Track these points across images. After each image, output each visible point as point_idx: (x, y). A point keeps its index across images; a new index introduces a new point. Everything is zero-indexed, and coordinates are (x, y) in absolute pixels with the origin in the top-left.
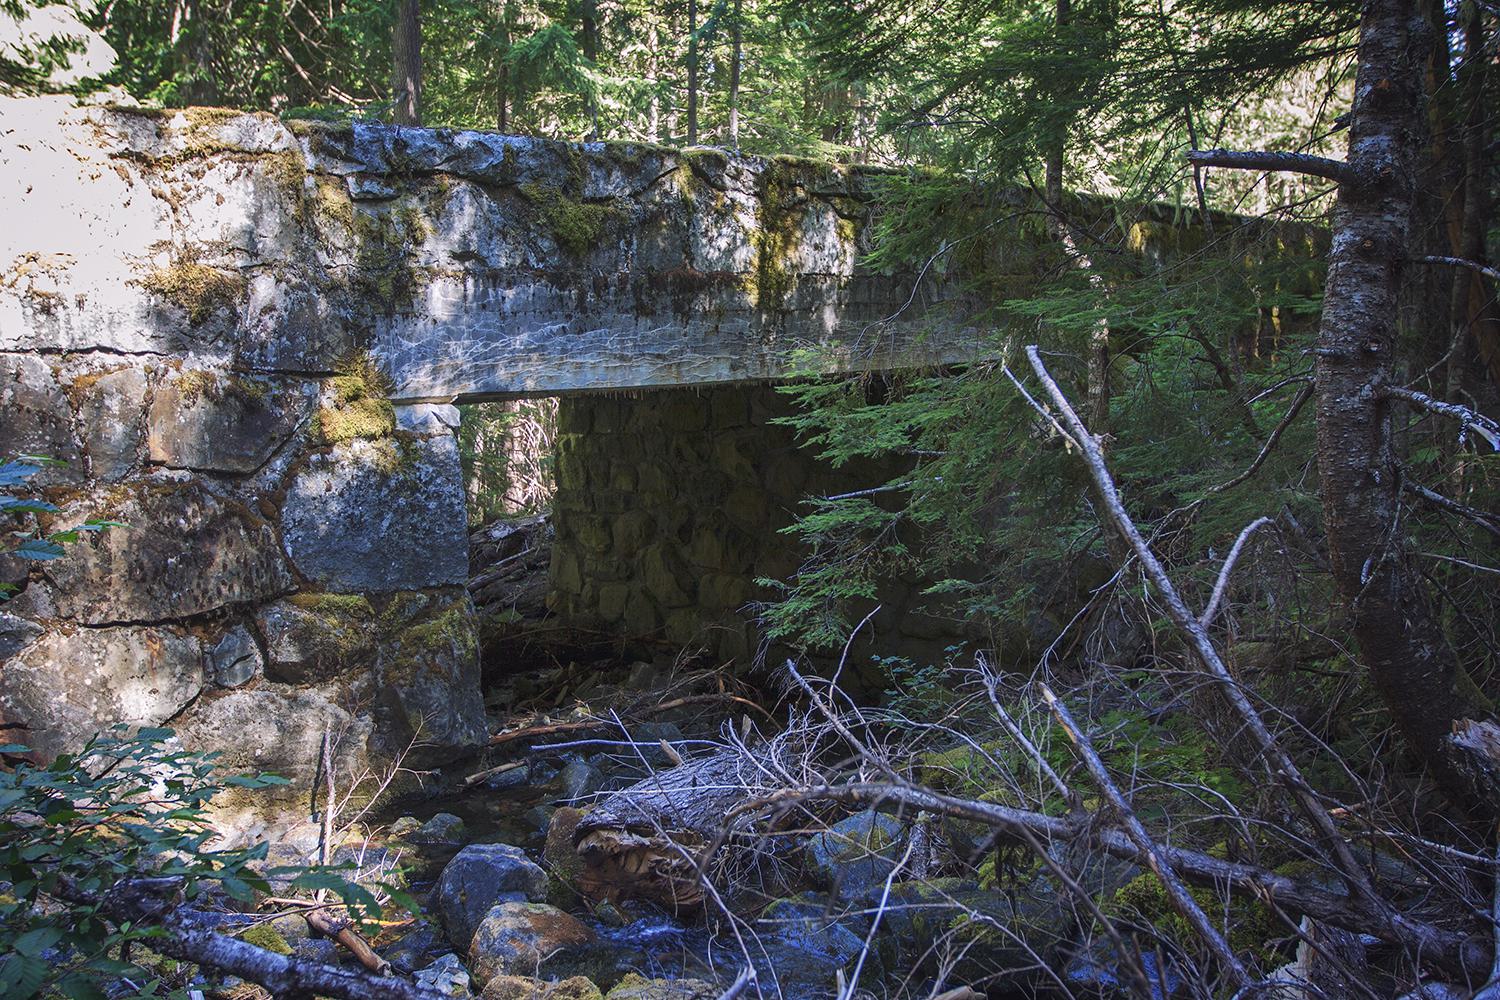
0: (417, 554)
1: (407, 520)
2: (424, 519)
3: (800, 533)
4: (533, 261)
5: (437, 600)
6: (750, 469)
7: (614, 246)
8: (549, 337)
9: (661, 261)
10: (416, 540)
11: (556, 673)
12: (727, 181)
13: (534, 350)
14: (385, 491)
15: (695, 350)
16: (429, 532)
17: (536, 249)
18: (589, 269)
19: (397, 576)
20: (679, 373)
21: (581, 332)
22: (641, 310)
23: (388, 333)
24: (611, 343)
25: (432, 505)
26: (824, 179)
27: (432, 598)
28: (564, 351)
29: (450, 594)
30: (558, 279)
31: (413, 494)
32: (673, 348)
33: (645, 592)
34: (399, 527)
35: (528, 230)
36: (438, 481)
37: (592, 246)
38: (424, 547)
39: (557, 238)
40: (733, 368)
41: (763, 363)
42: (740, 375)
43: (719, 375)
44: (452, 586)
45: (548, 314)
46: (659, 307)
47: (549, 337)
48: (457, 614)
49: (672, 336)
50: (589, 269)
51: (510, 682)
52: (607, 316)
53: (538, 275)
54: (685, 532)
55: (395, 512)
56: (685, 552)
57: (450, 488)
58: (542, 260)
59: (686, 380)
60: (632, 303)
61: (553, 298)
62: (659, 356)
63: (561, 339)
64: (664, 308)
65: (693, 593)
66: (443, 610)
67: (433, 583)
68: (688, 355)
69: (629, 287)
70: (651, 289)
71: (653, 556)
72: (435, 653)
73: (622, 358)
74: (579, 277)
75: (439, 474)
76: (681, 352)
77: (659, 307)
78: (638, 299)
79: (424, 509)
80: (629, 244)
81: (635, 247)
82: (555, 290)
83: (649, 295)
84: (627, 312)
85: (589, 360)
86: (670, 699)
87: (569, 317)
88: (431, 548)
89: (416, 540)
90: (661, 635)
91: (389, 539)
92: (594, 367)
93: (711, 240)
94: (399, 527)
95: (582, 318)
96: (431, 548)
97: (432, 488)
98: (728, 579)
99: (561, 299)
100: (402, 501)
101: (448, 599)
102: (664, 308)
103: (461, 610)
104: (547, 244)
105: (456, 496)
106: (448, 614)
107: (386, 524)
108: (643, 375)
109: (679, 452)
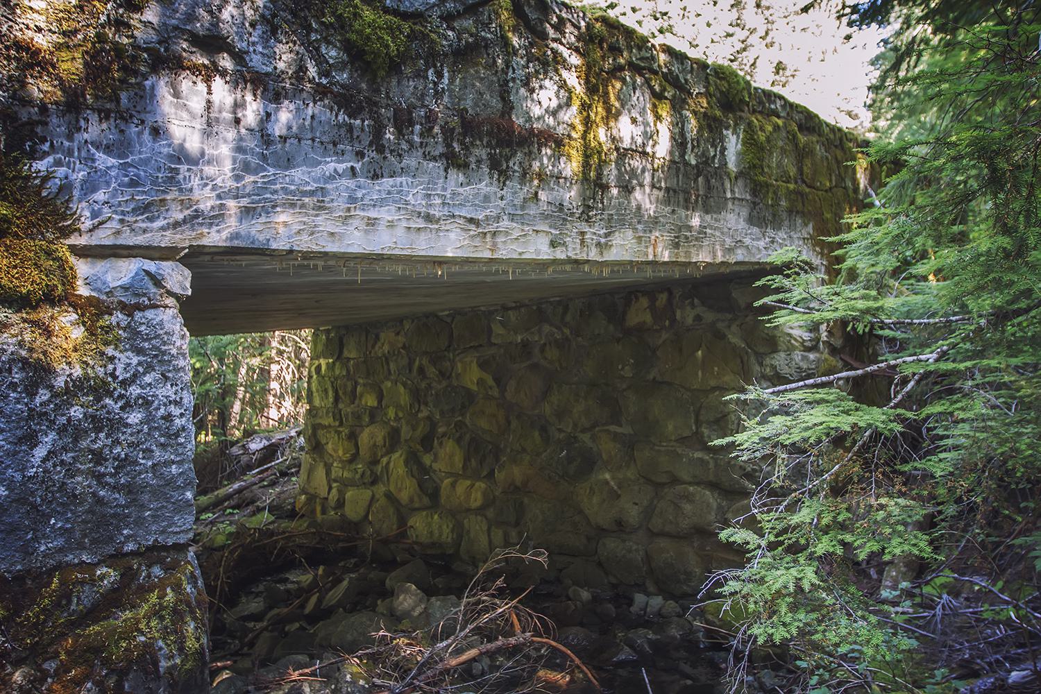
0: (99, 501)
1: (84, 444)
2: (117, 442)
3: (732, 446)
4: (312, 71)
5: (136, 574)
6: (491, 382)
7: (420, 75)
8: (331, 178)
9: (476, 105)
10: (99, 477)
11: (306, 578)
12: (551, 33)
13: (312, 193)
14: (43, 395)
15: (512, 217)
16: (124, 463)
17: (320, 60)
18: (388, 97)
19: (59, 542)
20: (495, 244)
21: (375, 176)
22: (453, 161)
23: (70, 137)
24: (415, 197)
25: (134, 418)
26: (640, 48)
27: (128, 575)
28: (352, 199)
29: (161, 561)
30: (345, 101)
31: (98, 399)
32: (488, 212)
33: (389, 496)
34: (68, 457)
35: (309, 29)
36: (148, 379)
37: (394, 67)
38: (115, 488)
39: (347, 46)
40: (553, 244)
41: (582, 241)
42: (560, 254)
43: (538, 252)
44: (165, 548)
45: (332, 147)
46: (473, 159)
47: (331, 178)
48: (170, 595)
49: (487, 198)
50: (388, 97)
51: (261, 588)
52: (410, 161)
53: (321, 92)
54: (427, 442)
55: (62, 431)
56: (427, 460)
57: (167, 391)
58: (326, 74)
59: (502, 254)
60: (440, 149)
61: (339, 126)
62: (471, 220)
63: (351, 183)
64: (479, 162)
65: (434, 495)
66: (144, 590)
67: (130, 547)
68: (505, 223)
69: (437, 130)
70: (464, 135)
71: (396, 462)
72: (122, 674)
73: (428, 218)
74: (376, 104)
75: (149, 368)
76: (498, 218)
77: (473, 159)
78: (449, 146)
79: (115, 425)
80: (440, 75)
81: (446, 81)
82: (342, 117)
83: (462, 143)
84: (434, 159)
85: (385, 214)
86: (458, 652)
87: (360, 155)
88: (129, 489)
89: (99, 477)
90: (403, 535)
91: (44, 479)
92: (391, 225)
93: (532, 91)
94: (68, 457)
95: (377, 159)
96: (129, 489)
97: (135, 391)
98: (468, 483)
99: (350, 129)
100: (76, 412)
101: (157, 571)
102: (479, 162)
103: (177, 588)
104: (333, 53)
105: (177, 403)
106: (153, 598)
107: (40, 452)
108: (452, 244)
109: (421, 370)
